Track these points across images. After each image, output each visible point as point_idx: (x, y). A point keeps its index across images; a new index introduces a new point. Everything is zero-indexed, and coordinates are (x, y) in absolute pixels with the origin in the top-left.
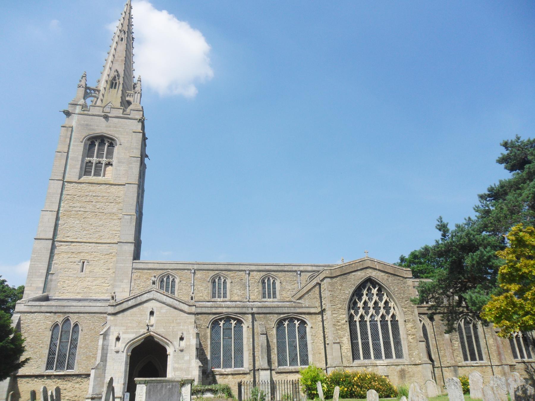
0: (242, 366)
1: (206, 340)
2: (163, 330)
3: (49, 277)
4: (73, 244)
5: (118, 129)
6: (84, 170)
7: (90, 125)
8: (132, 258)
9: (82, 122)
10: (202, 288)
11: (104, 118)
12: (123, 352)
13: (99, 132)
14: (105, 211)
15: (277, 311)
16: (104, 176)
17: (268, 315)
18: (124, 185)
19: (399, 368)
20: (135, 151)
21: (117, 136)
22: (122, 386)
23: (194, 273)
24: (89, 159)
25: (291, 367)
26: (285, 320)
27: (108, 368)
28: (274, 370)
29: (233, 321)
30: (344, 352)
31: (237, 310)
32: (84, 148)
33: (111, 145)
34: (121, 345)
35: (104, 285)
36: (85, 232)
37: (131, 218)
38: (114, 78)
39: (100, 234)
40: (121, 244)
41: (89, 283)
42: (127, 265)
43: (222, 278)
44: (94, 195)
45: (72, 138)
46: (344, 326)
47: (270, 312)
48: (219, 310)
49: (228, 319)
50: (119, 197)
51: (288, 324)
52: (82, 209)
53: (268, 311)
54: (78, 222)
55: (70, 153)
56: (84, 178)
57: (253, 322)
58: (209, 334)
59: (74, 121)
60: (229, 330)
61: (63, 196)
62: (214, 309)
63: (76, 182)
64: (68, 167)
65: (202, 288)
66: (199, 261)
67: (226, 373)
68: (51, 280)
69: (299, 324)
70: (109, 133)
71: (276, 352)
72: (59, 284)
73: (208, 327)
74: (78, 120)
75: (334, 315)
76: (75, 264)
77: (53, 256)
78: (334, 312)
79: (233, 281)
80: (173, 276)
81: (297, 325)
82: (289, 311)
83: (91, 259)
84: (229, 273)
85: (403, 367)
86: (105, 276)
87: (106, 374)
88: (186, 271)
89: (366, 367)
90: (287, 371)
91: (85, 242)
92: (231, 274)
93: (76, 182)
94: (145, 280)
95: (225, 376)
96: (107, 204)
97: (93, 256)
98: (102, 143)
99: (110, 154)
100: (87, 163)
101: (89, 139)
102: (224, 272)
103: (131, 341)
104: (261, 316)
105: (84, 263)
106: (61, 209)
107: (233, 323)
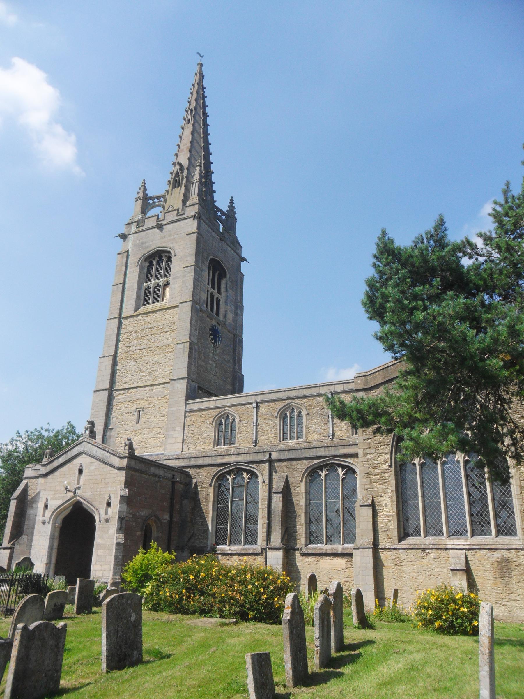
0: (256, 544)
1: (208, 504)
2: (90, 493)
3: (108, 433)
4: (130, 391)
5: (172, 237)
6: (142, 298)
7: (146, 243)
8: (185, 398)
9: (138, 242)
10: (268, 428)
11: (158, 228)
12: (49, 523)
13: (153, 247)
14: (161, 344)
15: (307, 455)
16: (163, 300)
17: (294, 463)
18: (176, 306)
19: (497, 555)
20: (189, 258)
21: (171, 246)
22: (45, 566)
23: (257, 407)
24: (147, 284)
25: (329, 546)
26: (321, 468)
27: (34, 543)
28: (298, 550)
29: (245, 474)
30: (382, 523)
31: (250, 458)
32: (140, 273)
33: (169, 259)
34: (48, 513)
35: (160, 436)
36: (141, 374)
37: (184, 347)
38: (177, 175)
39: (156, 373)
40: (174, 382)
41: (145, 436)
42: (180, 408)
43: (295, 410)
44: (149, 327)
45: (129, 264)
46: (387, 474)
47: (297, 456)
48: (226, 459)
49: (238, 471)
50: (174, 323)
51: (326, 475)
52: (138, 347)
53: (293, 456)
54: (134, 364)
55: (127, 283)
56: (143, 309)
57: (270, 475)
58: (211, 495)
59: (130, 244)
60: (240, 488)
61: (121, 335)
62: (219, 457)
63: (132, 316)
64: (125, 300)
65: (268, 428)
66: (265, 389)
67: (229, 552)
68: (110, 437)
69: (344, 474)
70: (164, 245)
71: (303, 521)
72: (117, 441)
73: (210, 485)
74: (133, 241)
75: (369, 456)
76: (131, 414)
77: (112, 409)
78: (368, 451)
79: (310, 411)
80: (232, 415)
81: (341, 476)
82: (327, 453)
83: (146, 406)
84: (304, 400)
85: (506, 554)
86: (160, 425)
87: (32, 551)
88: (248, 406)
89: (424, 550)
90: (318, 552)
91: (141, 387)
92: (308, 402)
93: (132, 316)
94: (200, 424)
95: (228, 557)
96: (162, 334)
97: (148, 402)
98: (160, 261)
99: (168, 270)
100: (146, 289)
101: (145, 260)
102: (297, 401)
103: (57, 509)
104: (283, 464)
105: (139, 411)
106: (119, 351)
107: (245, 476)
